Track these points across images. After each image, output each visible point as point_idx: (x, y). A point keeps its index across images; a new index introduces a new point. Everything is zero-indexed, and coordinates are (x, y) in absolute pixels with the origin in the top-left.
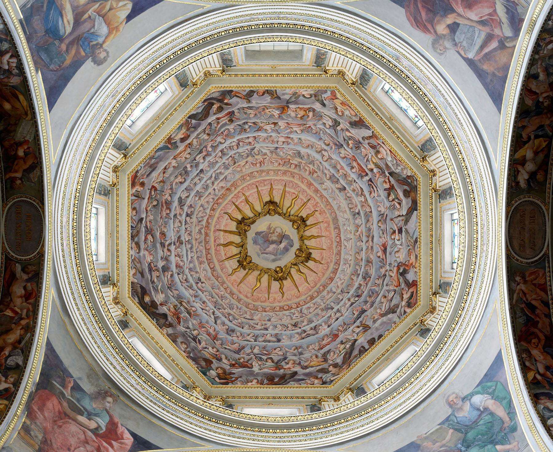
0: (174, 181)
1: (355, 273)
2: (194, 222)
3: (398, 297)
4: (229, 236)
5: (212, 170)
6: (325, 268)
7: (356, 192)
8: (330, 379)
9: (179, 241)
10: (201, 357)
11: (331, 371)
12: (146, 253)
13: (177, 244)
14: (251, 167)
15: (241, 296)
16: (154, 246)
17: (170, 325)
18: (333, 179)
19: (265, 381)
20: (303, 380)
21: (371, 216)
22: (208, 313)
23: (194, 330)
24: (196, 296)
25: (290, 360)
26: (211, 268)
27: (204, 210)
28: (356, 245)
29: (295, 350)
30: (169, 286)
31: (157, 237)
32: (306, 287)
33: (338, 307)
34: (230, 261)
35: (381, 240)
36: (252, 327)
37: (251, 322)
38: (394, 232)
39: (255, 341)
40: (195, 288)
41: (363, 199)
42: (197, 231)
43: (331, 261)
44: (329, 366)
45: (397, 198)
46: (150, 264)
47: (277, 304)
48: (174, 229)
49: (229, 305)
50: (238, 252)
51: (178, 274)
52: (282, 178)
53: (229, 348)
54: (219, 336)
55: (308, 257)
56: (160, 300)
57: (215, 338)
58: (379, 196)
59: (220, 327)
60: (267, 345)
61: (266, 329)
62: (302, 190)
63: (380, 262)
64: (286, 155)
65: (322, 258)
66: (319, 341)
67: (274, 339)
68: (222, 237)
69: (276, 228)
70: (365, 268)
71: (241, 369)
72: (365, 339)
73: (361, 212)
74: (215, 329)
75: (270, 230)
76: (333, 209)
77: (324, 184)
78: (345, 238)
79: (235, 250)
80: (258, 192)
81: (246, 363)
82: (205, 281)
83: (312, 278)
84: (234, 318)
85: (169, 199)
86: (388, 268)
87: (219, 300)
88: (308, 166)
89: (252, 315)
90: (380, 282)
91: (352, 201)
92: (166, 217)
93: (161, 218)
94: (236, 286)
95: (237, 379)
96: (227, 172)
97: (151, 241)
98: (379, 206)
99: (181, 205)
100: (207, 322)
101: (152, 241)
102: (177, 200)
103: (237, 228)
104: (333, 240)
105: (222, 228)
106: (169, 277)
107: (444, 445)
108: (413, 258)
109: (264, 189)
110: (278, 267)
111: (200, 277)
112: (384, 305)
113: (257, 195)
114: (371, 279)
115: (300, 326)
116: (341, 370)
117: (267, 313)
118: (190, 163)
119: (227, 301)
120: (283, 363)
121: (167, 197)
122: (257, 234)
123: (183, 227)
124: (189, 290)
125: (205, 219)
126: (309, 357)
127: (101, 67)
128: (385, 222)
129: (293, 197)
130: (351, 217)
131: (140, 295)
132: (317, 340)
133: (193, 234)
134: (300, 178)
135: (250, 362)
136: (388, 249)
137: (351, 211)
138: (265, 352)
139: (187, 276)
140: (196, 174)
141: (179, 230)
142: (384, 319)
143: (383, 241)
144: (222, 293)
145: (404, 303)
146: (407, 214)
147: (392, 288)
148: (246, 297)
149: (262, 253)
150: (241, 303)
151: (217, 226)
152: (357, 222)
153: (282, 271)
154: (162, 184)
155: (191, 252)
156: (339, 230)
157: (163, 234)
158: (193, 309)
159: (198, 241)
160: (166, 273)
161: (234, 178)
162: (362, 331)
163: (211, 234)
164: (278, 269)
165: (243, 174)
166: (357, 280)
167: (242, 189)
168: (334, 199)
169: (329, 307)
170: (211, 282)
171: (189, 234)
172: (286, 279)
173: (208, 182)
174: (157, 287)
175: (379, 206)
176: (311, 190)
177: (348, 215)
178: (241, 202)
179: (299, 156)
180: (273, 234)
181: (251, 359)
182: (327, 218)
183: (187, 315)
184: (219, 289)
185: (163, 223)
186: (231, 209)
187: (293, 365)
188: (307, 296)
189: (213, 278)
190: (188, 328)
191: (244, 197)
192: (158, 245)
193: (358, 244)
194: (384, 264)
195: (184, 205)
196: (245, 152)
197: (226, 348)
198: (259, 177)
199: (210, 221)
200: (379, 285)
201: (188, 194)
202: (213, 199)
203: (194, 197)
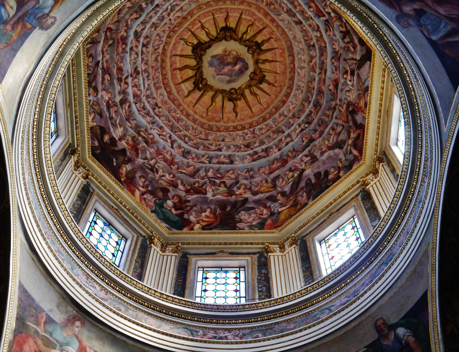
0: (129, 18)
1: (307, 100)
2: (151, 51)
3: (346, 133)
5: (168, 4)
6: (278, 91)
7: (312, 28)
8: (277, 210)
9: (136, 72)
10: (158, 188)
11: (279, 200)
12: (104, 93)
13: (134, 75)
15: (197, 117)
16: (112, 83)
17: (130, 161)
18: (289, 12)
19: (218, 210)
20: (253, 208)
21: (326, 51)
22: (165, 138)
23: (152, 159)
24: (153, 123)
25: (241, 185)
26: (167, 92)
28: (309, 74)
29: (246, 173)
30: (127, 117)
31: (113, 74)
32: (259, 108)
35: (333, 75)
36: (207, 147)
37: (206, 143)
38: (346, 72)
39: (210, 163)
41: (318, 34)
42: (153, 59)
43: (285, 85)
44: (278, 194)
45: (352, 42)
46: (108, 103)
47: (230, 124)
49: (186, 127)
50: (194, 74)
51: (136, 103)
52: (239, 7)
53: (185, 171)
54: (176, 160)
55: (262, 80)
56: (118, 135)
57: (171, 163)
58: (334, 35)
59: (176, 151)
60: (220, 167)
61: (220, 150)
62: (258, 18)
63: (331, 95)
65: (276, 81)
66: (269, 164)
67: (227, 161)
68: (178, 62)
70: (316, 96)
71: (195, 196)
72: (312, 171)
73: (316, 45)
74: (171, 154)
75: (226, 53)
76: (289, 38)
78: (299, 66)
79: (190, 73)
80: (214, 19)
81: (200, 189)
82: (161, 106)
83: (265, 100)
84: (190, 139)
85: (125, 34)
86: (338, 102)
87: (176, 123)
89: (207, 135)
90: (330, 113)
92: (122, 52)
93: (117, 54)
94: (192, 107)
95: (192, 208)
97: (108, 80)
98: (333, 44)
100: (164, 148)
101: (109, 79)
102: (133, 34)
104: (288, 65)
105: (178, 53)
106: (127, 108)
108: (362, 104)
109: (220, 17)
110: (233, 89)
111: (157, 102)
112: (332, 137)
113: (213, 21)
114: (322, 109)
115: (252, 147)
116: (288, 200)
117: (222, 133)
120: (235, 189)
121: (123, 33)
122: (213, 57)
125: (161, 47)
126: (259, 182)
127: (49, 31)
128: (339, 61)
130: (305, 48)
131: (99, 136)
132: (268, 163)
133: (149, 63)
134: (256, 8)
135: (204, 187)
136: (340, 86)
138: (219, 175)
139: (144, 103)
140: (151, 9)
141: (135, 61)
142: (331, 153)
143: (334, 76)
144: (179, 116)
145: (350, 142)
146: (360, 60)
147: (340, 122)
148: (202, 117)
149: (217, 75)
150: (197, 123)
151: (174, 52)
152: (311, 53)
154: (117, 23)
155: (148, 80)
157: (120, 70)
158: (151, 136)
159: (154, 68)
160: (124, 106)
161: (190, 7)
162: (310, 161)
163: (168, 60)
164: (233, 91)
165: (200, 4)
167: (199, 16)
168: (290, 30)
169: (280, 130)
170: (167, 106)
171: (146, 64)
172: (240, 99)
173: (164, 14)
174: (116, 121)
175: (333, 44)
177: (303, 45)
180: (229, 57)
181: (205, 183)
182: (282, 45)
183: (145, 145)
184: (175, 112)
185: (119, 59)
186: (187, 35)
187: (244, 191)
188: (259, 116)
189: (169, 102)
190: (146, 158)
191: (200, 24)
192: (115, 82)
193: (311, 73)
194: (334, 97)
195: (140, 37)
197: (181, 173)
198: (215, 6)
199: (166, 48)
200: (328, 116)
201: (144, 26)
202: (169, 28)
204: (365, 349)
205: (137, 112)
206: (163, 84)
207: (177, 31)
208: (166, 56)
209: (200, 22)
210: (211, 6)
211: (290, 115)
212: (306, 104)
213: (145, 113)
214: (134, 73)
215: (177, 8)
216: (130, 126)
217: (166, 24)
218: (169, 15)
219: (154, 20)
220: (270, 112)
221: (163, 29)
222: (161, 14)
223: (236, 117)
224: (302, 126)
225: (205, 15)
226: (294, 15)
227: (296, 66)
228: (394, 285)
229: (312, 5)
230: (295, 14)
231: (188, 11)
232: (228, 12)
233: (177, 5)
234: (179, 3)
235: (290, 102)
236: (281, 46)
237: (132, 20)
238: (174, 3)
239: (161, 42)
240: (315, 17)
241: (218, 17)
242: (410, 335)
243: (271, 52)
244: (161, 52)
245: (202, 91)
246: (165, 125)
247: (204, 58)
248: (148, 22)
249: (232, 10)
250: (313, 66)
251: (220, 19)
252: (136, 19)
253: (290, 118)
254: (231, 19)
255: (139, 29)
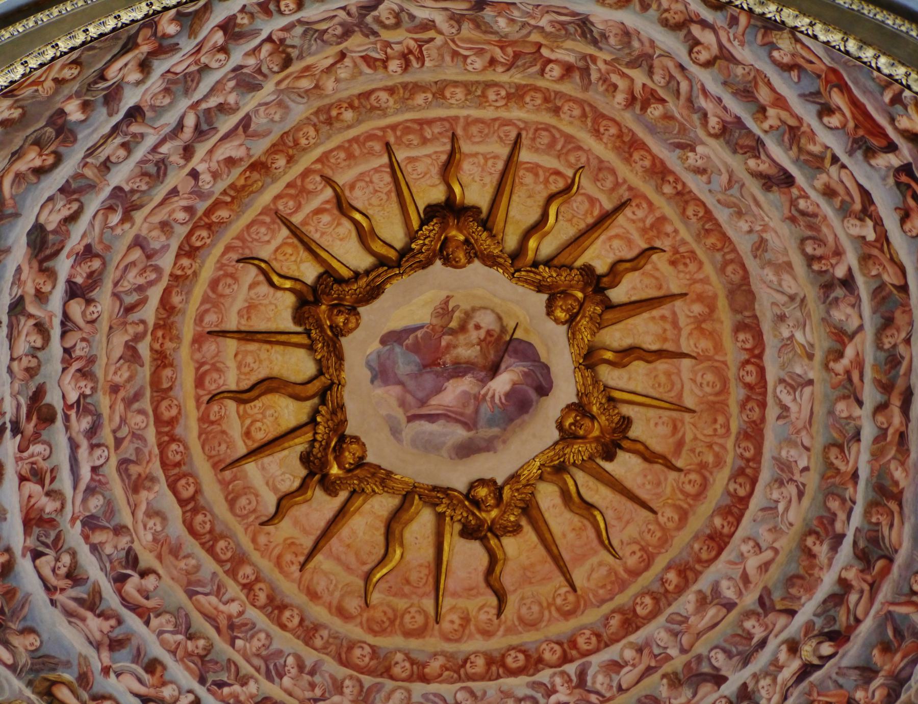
2: (105, 316)
4: (263, 355)
5: (184, 104)
6: (689, 488)
7: (837, 202)
13: (30, 428)
14: (361, 73)
15: (319, 613)
24: (115, 645)
26: (182, 502)
27: (149, 257)
28: (831, 412)
32: (603, 571)
33: (745, 675)
34: (267, 460)
40: (111, 599)
42: (118, 351)
43: (719, 462)
47: (474, 644)
48: (15, 365)
49: (266, 660)
50: (304, 418)
51: (36, 555)
52: (504, 114)
62: (594, 163)
64: (524, 32)
65: (680, 444)
68: (232, 364)
69: (474, 310)
70: (867, 513)
73: (860, 280)
76: (734, 250)
77: (693, 150)
78: (782, 374)
80: (393, 168)
83: (632, 531)
87: (221, 645)
88: (623, 75)
91: (818, 230)
94: (295, 568)
96: (249, 103)
99: (42, 255)
102: (24, 240)
103: (298, 318)
104: (732, 373)
105: (232, 324)
110: (482, 482)
111: (136, 546)
113: (388, 178)
114: (895, 569)
117: (434, 687)
118: (78, 94)
119: (256, 643)
122: (392, 338)
123: (56, 347)
124: (83, 620)
125: (155, 295)
129: (553, 189)
130: (812, 293)
133: (99, 370)
134: (584, 115)
137: (816, 267)
139: (73, 554)
140: (107, 129)
141: (34, 363)
144: (234, 608)
148: (341, 613)
149: (411, 419)
150: (318, 642)
151: (211, 319)
152: (837, 315)
153: (499, 499)
155: (93, 447)
156: (758, 336)
159: (122, 394)
161: (282, 119)
163: (184, 356)
164: (482, 492)
165: (327, 101)
166: (831, 560)
168: (740, 214)
169: (705, 668)
170: (182, 564)
171: (85, 373)
172: (516, 529)
173: (164, 149)
176: (638, 167)
178: (318, 211)
179: (583, 35)
180: (462, 338)
182: (706, 281)
184: (219, 591)
188: (606, 608)
189: (191, 545)
191: (329, 193)
195: (57, 253)
196: (336, 20)
198: (397, 112)
199: (176, 299)
201: (75, 206)
202: (190, 210)
203: (100, 217)
205: (39, 595)
206: (164, 465)
207: (224, 224)
208: (178, 339)
209: (329, 181)
210: (383, 111)
211: (750, 599)
212: (822, 550)
213: (80, 601)
214: (29, 418)
215: (226, 124)
216: (10, 661)
217: (174, 192)
218: (188, 152)
219: (120, 176)
220: (656, 587)
221: (162, 215)
222: (154, 149)
223: (500, 612)
224: (807, 651)
225: (349, 151)
226: (756, 148)
227: (771, 375)
229: (837, 99)
230: (759, 141)
231: (273, 138)
232: (454, 138)
233: (222, 108)
234: (232, 99)
235: (746, 540)
236: (698, 287)
237: (19, 176)
238: (213, 102)
239: (153, 276)
240: (851, 153)
241: (412, 160)
243: (656, 313)
244: (151, 322)
245: (343, 495)
246: (173, 653)
247: (347, 343)
248: (92, 187)
249: (474, 130)
250: (848, 373)
251: (421, 167)
252: (40, 172)
253: (748, 614)
254: (467, 167)
255: (52, 221)
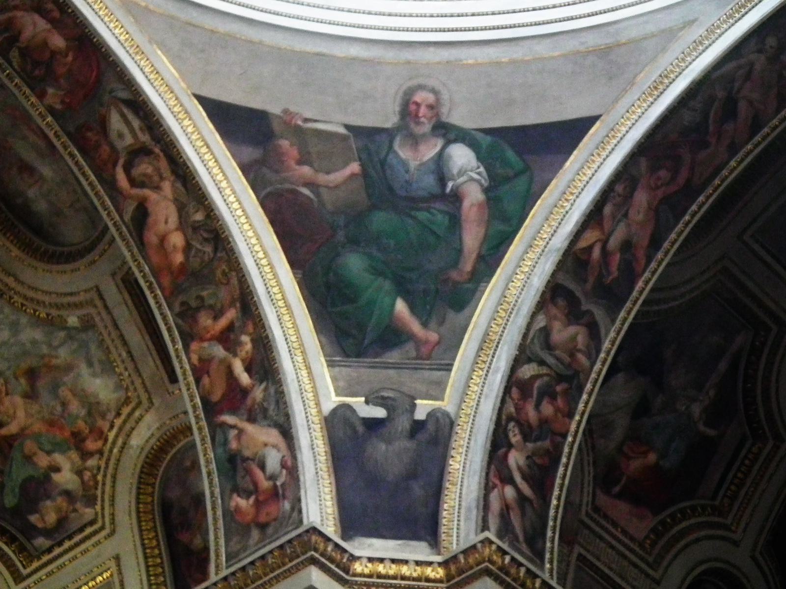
107: (318, 186)
204: (342, 130)
228: (528, 42)
242: (478, 181)
